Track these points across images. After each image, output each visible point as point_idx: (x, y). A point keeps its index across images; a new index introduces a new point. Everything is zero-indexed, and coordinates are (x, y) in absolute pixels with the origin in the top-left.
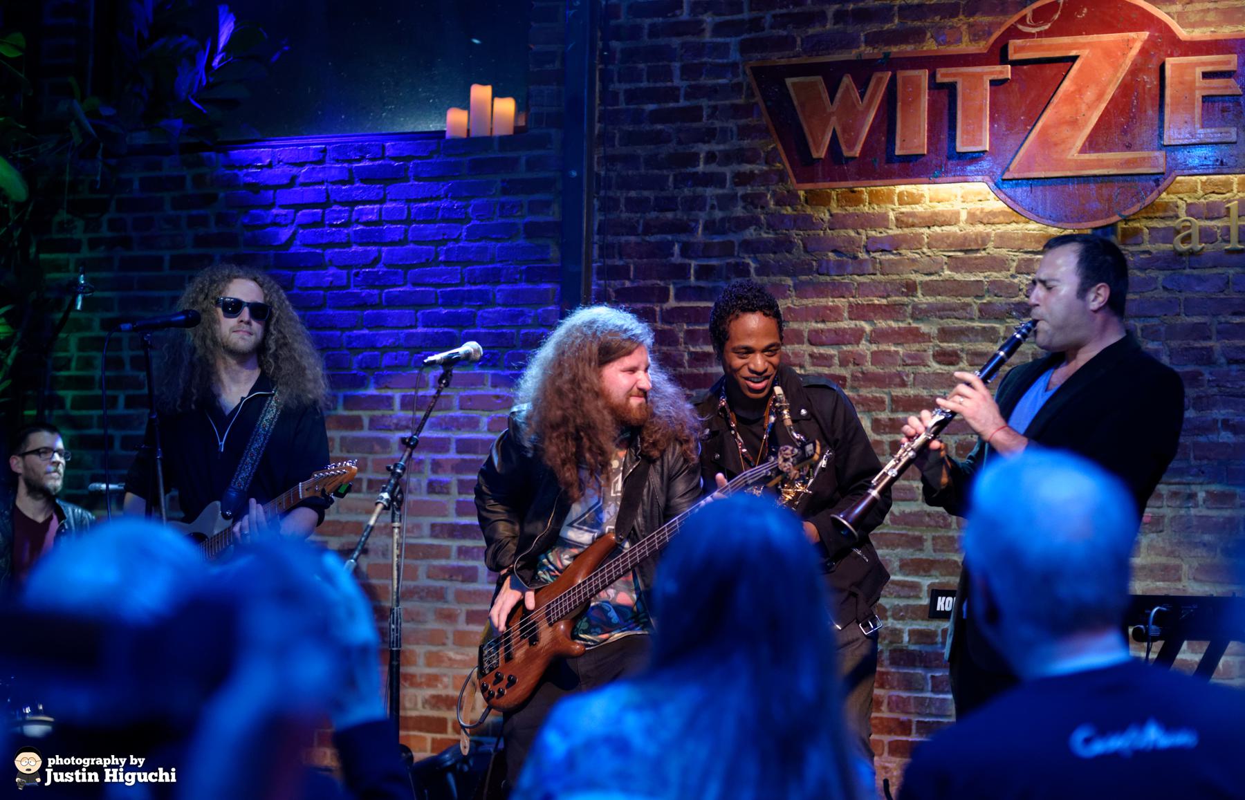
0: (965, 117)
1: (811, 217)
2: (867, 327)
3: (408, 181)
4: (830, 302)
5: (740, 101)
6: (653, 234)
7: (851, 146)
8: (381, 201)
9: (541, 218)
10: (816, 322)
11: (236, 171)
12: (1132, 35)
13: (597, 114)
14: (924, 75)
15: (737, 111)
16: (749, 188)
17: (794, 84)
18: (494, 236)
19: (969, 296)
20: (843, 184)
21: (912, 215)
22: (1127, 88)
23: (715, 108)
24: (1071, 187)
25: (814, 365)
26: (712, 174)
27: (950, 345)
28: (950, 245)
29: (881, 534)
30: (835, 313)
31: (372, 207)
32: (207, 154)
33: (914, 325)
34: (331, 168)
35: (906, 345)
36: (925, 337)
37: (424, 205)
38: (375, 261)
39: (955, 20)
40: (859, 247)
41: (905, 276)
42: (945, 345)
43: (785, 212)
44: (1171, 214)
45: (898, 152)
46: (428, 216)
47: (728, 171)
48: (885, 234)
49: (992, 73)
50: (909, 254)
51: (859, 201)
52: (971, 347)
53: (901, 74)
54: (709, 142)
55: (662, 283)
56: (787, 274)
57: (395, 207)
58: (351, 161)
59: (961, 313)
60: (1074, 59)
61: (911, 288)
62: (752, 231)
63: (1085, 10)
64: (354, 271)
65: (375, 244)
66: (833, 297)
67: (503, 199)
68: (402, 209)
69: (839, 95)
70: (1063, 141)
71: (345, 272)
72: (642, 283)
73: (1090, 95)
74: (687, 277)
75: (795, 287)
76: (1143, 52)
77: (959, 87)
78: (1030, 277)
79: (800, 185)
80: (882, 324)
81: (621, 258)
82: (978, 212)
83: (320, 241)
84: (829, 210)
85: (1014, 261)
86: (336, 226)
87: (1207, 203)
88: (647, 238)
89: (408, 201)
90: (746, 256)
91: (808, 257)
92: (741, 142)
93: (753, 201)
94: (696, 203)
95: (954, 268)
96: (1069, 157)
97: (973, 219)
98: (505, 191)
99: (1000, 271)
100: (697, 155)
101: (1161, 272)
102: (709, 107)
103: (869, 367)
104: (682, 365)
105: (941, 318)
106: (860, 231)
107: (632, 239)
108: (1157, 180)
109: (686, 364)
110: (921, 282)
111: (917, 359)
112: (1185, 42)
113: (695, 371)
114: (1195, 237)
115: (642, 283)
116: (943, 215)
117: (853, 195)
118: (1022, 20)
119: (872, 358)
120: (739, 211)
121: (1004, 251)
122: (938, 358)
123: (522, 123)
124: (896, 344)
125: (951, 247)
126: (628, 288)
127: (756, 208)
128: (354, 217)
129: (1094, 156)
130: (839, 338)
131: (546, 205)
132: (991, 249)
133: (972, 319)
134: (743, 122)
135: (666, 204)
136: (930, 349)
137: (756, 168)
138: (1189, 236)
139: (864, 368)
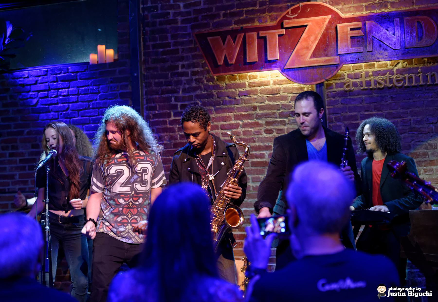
0: (270, 48)
1: (219, 85)
2: (241, 123)
3: (77, 80)
4: (227, 114)
5: (193, 46)
6: (164, 94)
7: (231, 60)
8: (68, 88)
9: (125, 91)
10: (223, 122)
11: (16, 80)
12: (326, 17)
13: (142, 54)
14: (255, 34)
15: (191, 50)
16: (197, 76)
17: (210, 39)
18: (109, 98)
19: (275, 110)
20: (229, 73)
21: (254, 83)
22: (325, 35)
23: (183, 49)
24: (308, 71)
25: (223, 137)
26: (184, 72)
27: (270, 127)
28: (268, 93)
29: (250, 194)
30: (229, 118)
31: (65, 90)
32: (5, 74)
33: (257, 121)
34: (50, 77)
35: (254, 128)
36: (260, 125)
37: (84, 88)
38: (67, 109)
39: (265, 14)
40: (236, 95)
41: (253, 104)
42: (268, 127)
43: (210, 84)
44: (342, 78)
45: (248, 61)
46: (86, 92)
47: (189, 71)
48: (245, 90)
49: (278, 32)
50: (254, 96)
51: (235, 79)
52: (277, 128)
53: (248, 34)
54: (182, 61)
55: (168, 111)
56: (212, 106)
57: (73, 90)
58: (57, 74)
59: (273, 116)
60: (306, 26)
61: (255, 108)
62: (199, 91)
63: (309, 9)
64: (60, 113)
65: (66, 103)
66: (228, 113)
67: (111, 85)
68: (75, 90)
69: (226, 42)
70: (304, 55)
71: (57, 113)
72: (162, 111)
73: (312, 38)
74: (177, 108)
75: (215, 110)
76: (330, 22)
77: (268, 38)
79: (214, 74)
80: (246, 121)
81: (154, 103)
82: (276, 81)
83: (47, 103)
84: (225, 83)
85: (290, 97)
86: (53, 97)
87: (354, 74)
88: (163, 96)
89: (78, 87)
90: (197, 100)
91: (219, 99)
92: (193, 61)
93: (199, 81)
94: (179, 83)
95: (270, 100)
96: (307, 60)
97: (275, 83)
98: (112, 82)
99: (285, 101)
100: (178, 66)
101: (340, 98)
102: (181, 49)
103: (242, 136)
104: (177, 139)
105: (266, 118)
106: (236, 89)
107: (157, 96)
108: (337, 66)
109: (179, 139)
110: (258, 106)
111: (258, 133)
112: (344, 18)
113: (182, 141)
114: (351, 85)
115: (162, 111)
116: (264, 82)
117: (233, 77)
118: (288, 13)
119: (243, 133)
120: (194, 85)
121: (286, 94)
122: (266, 132)
123: (116, 58)
124: (251, 128)
125: (267, 93)
126: (157, 114)
127: (200, 83)
128: (59, 93)
129: (315, 59)
130: (231, 127)
131: (127, 86)
132: (282, 93)
133: (276, 118)
134: (193, 53)
135: (169, 83)
136: (263, 129)
137: (199, 69)
138: (349, 85)
139: (240, 137)
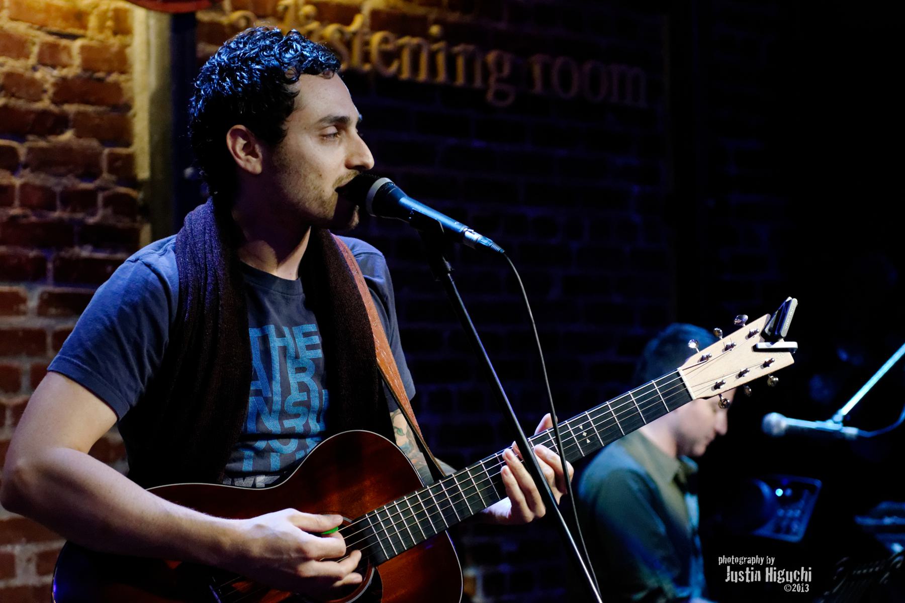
78: (56, 73)
85: (34, 44)
